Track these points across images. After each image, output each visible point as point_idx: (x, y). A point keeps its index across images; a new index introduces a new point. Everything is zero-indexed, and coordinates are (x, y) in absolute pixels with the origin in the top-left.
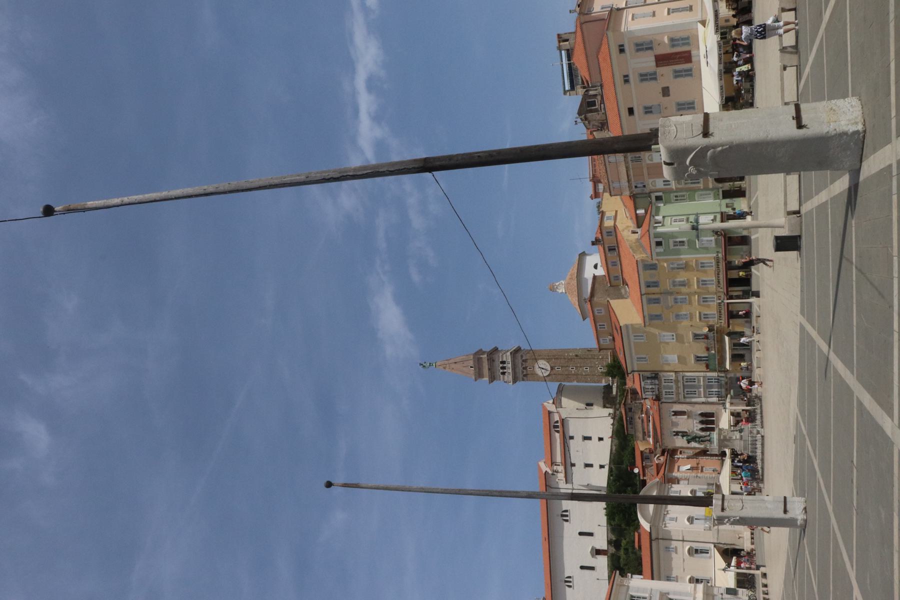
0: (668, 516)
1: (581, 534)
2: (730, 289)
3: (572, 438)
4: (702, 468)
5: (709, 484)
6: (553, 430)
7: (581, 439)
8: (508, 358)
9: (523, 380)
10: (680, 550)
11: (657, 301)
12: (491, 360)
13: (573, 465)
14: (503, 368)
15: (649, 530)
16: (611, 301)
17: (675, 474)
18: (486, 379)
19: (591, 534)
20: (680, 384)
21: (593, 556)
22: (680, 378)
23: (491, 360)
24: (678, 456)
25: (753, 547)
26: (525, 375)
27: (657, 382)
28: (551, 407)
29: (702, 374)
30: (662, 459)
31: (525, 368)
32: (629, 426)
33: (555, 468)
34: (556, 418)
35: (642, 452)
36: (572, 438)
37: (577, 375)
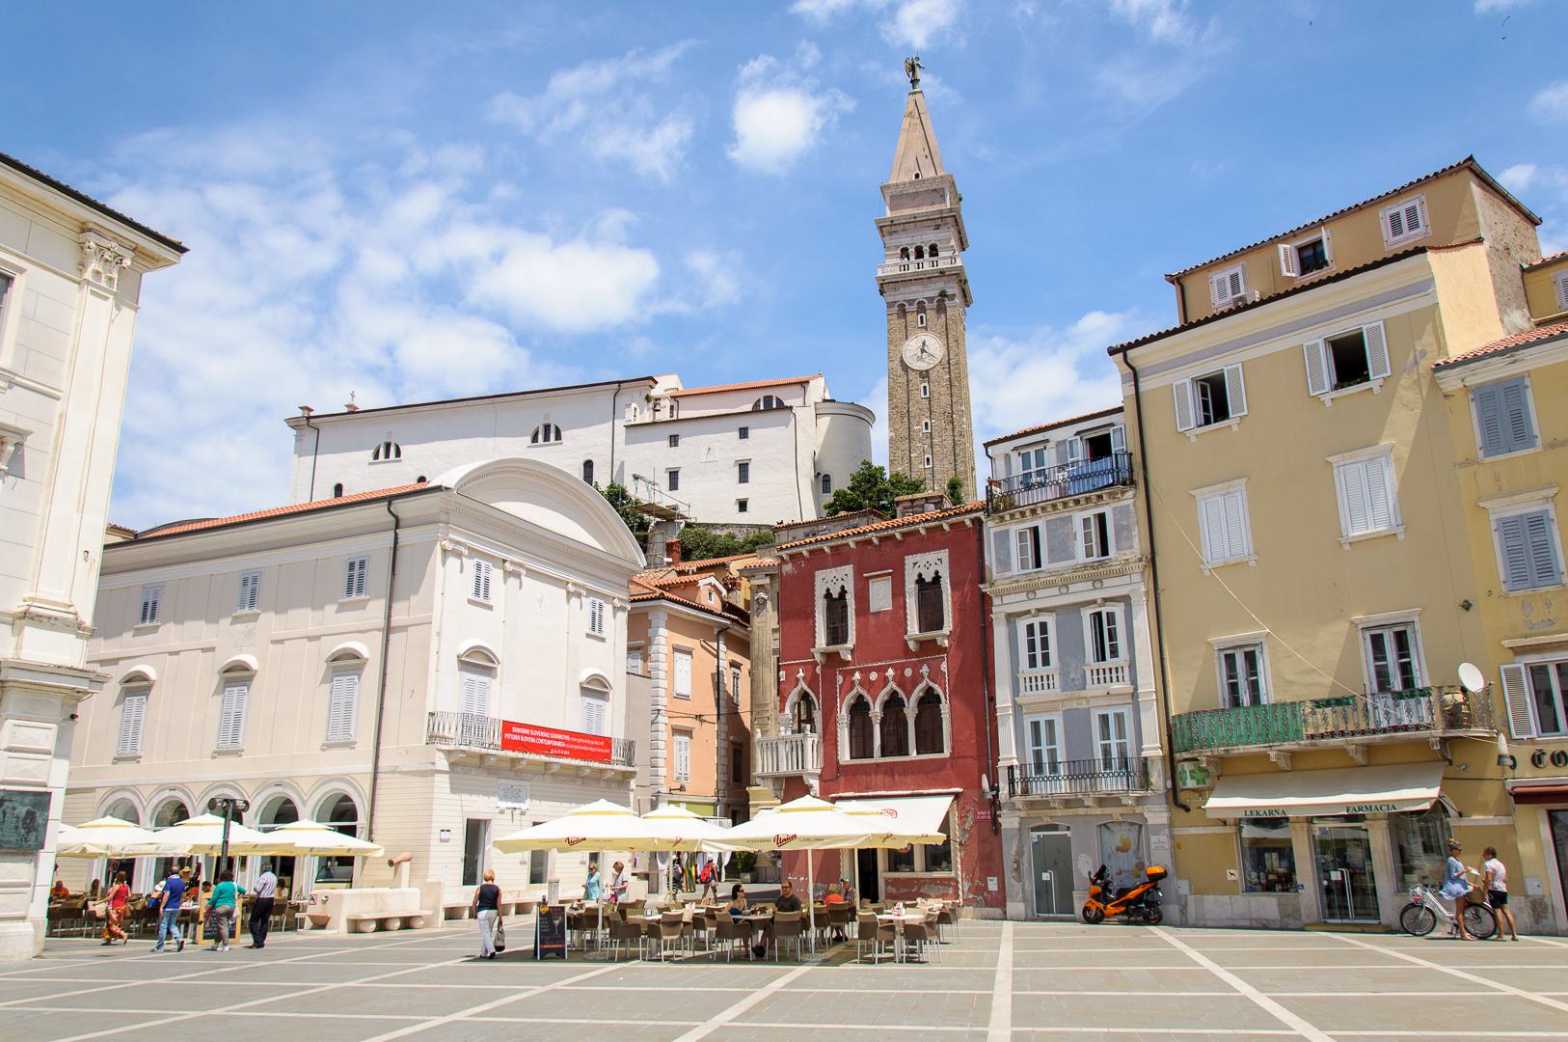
0: (496, 574)
3: (744, 433)
4: (688, 733)
5: (629, 747)
7: (742, 456)
9: (890, 305)
10: (351, 619)
12: (938, 222)
13: (674, 440)
14: (919, 254)
16: (1480, 250)
17: (664, 638)
18: (889, 214)
20: (1081, 592)
22: (1113, 587)
23: (938, 222)
24: (727, 655)
25: (339, 930)
26: (903, 312)
28: (817, 390)
29: (1147, 684)
30: (715, 604)
31: (921, 308)
33: (666, 403)
35: (724, 566)
36: (744, 433)
37: (910, 438)
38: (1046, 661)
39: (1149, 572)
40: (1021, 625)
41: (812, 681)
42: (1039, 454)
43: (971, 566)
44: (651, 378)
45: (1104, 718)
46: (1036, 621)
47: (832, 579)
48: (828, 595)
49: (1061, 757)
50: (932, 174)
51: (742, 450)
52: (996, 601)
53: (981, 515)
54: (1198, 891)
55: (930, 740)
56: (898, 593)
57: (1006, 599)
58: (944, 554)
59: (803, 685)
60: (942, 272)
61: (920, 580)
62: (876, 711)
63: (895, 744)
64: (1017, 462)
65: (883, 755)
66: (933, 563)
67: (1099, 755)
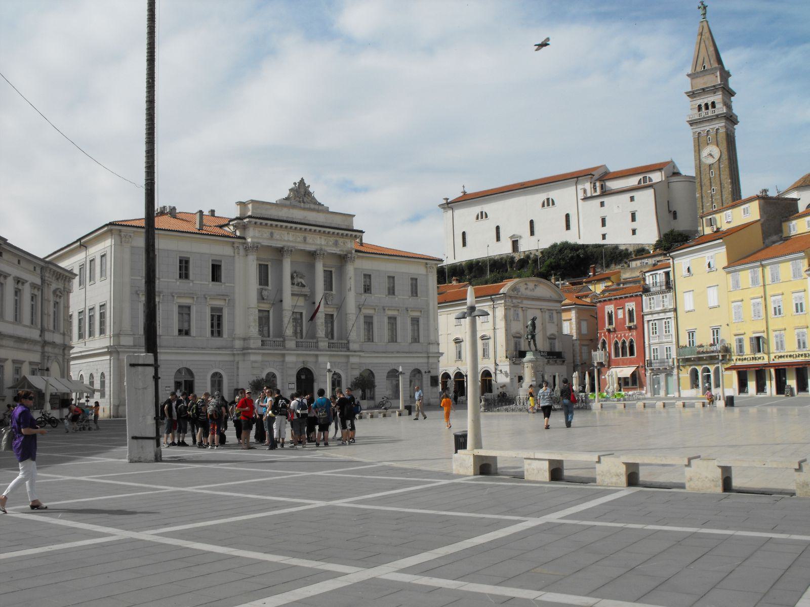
1: (532, 222)
2: (773, 370)
6: (641, 177)
8: (721, 109)
9: (694, 133)
11: (754, 281)
14: (707, 107)
15: (501, 291)
19: (532, 233)
21: (511, 237)
23: (714, 90)
27: (664, 287)
29: (674, 340)
32: (638, 263)
33: (598, 184)
34: (656, 177)
36: (632, 199)
38: (656, 334)
39: (675, 313)
40: (651, 323)
41: (605, 336)
42: (656, 276)
43: (640, 306)
44: (591, 174)
45: (667, 348)
46: (654, 322)
47: (610, 308)
48: (608, 313)
49: (659, 358)
50: (710, 67)
51: (633, 206)
52: (645, 317)
53: (641, 293)
54: (682, 389)
55: (632, 353)
56: (624, 314)
57: (648, 316)
58: (634, 303)
59: (603, 338)
60: (717, 116)
61: (629, 310)
62: (620, 345)
63: (624, 354)
64: (651, 277)
65: (630, 356)
66: (631, 305)
67: (666, 357)
